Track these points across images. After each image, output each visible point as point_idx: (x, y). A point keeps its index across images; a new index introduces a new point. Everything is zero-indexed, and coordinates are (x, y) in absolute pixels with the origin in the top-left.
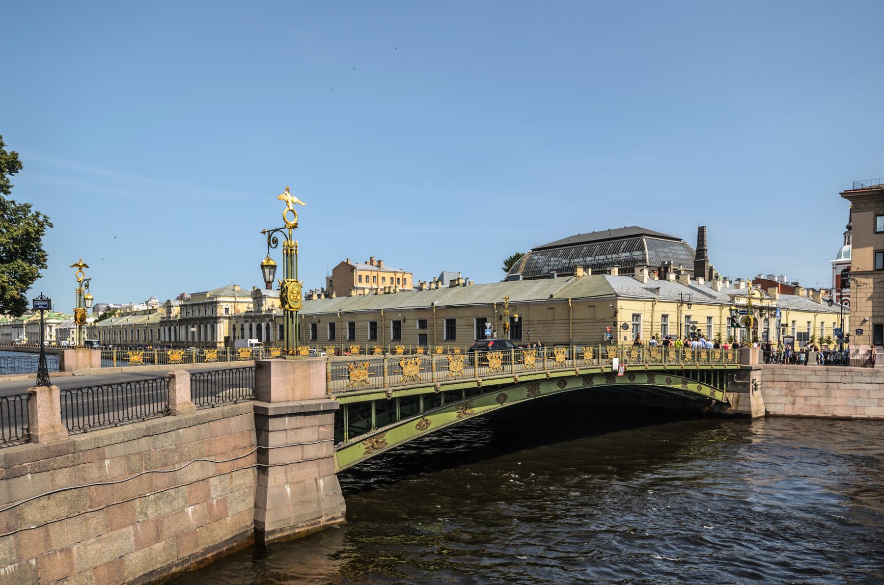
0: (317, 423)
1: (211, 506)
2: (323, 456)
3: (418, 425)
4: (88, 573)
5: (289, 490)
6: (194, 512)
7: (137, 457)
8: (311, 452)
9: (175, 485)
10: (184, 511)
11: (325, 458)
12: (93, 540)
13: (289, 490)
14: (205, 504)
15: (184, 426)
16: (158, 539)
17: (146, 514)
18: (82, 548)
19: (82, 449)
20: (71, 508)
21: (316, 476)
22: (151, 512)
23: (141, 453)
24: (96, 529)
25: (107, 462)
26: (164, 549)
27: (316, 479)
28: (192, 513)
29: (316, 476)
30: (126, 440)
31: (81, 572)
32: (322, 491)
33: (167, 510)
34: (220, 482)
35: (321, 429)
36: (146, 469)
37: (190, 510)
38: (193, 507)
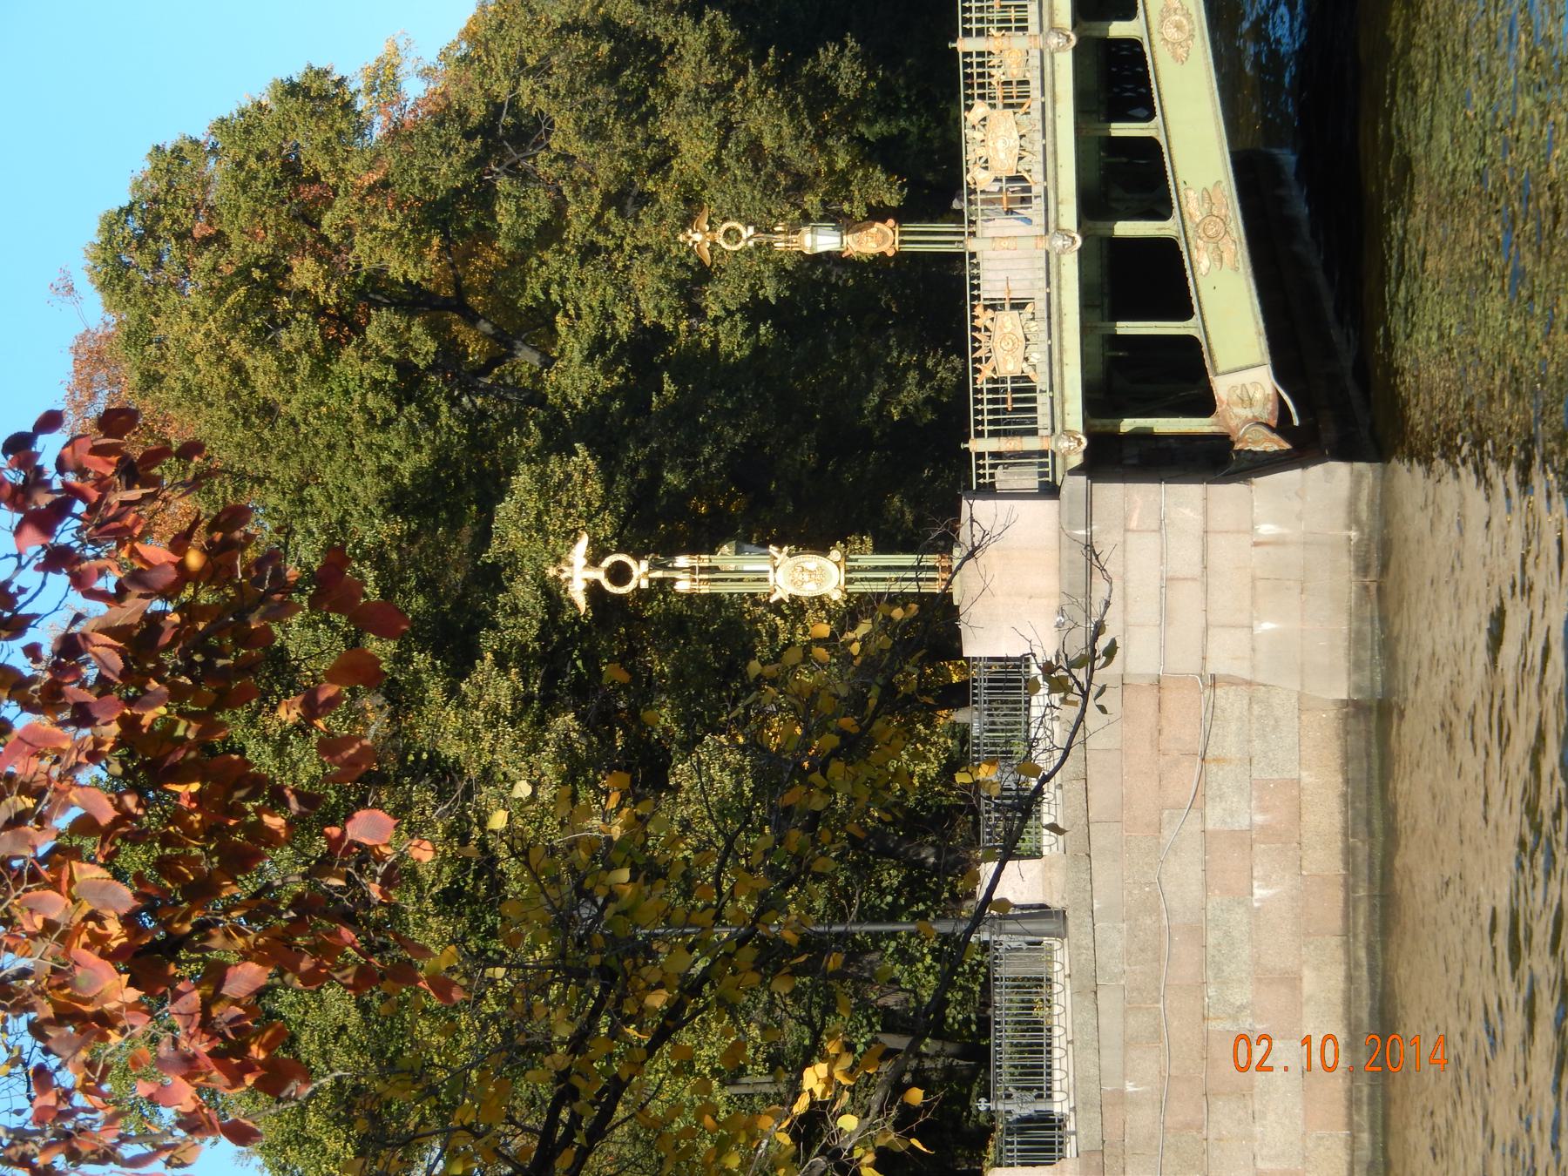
0: (1116, 537)
1: (1263, 828)
2: (1200, 518)
3: (1176, 57)
4: (1310, 1145)
5: (1267, 626)
6: (1267, 881)
7: (1131, 1020)
8: (1185, 557)
9: (1197, 932)
10: (1259, 909)
11: (1206, 513)
12: (1257, 1129)
13: (1267, 626)
14: (1258, 847)
15: (1088, 896)
16: (1292, 981)
17: (1242, 1008)
18: (1265, 1151)
19: (1098, 1138)
20: (1194, 1166)
21: (1246, 541)
22: (1240, 995)
23: (1125, 1011)
24: (1240, 1122)
25: (1130, 1087)
26: (1317, 969)
27: (1256, 544)
28: (1267, 886)
29: (1246, 541)
30: (1095, 1044)
31: (1305, 1157)
32: (1286, 531)
33: (1245, 952)
34: (1221, 797)
35: (1133, 524)
36: (1157, 1002)
37: (1259, 892)
38: (1255, 884)
